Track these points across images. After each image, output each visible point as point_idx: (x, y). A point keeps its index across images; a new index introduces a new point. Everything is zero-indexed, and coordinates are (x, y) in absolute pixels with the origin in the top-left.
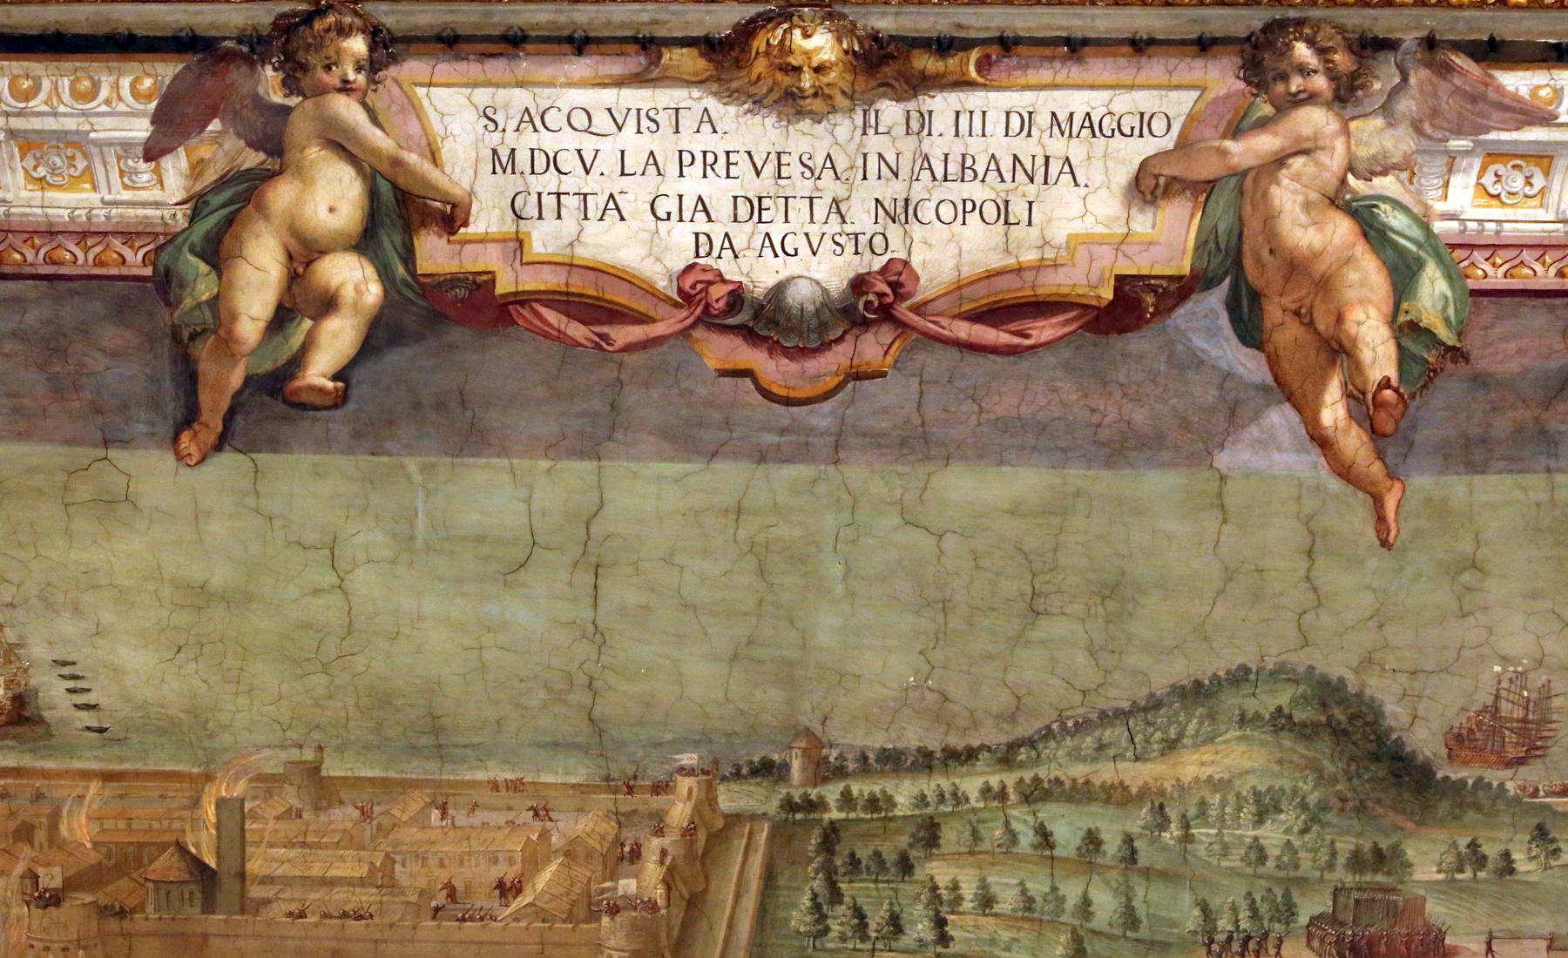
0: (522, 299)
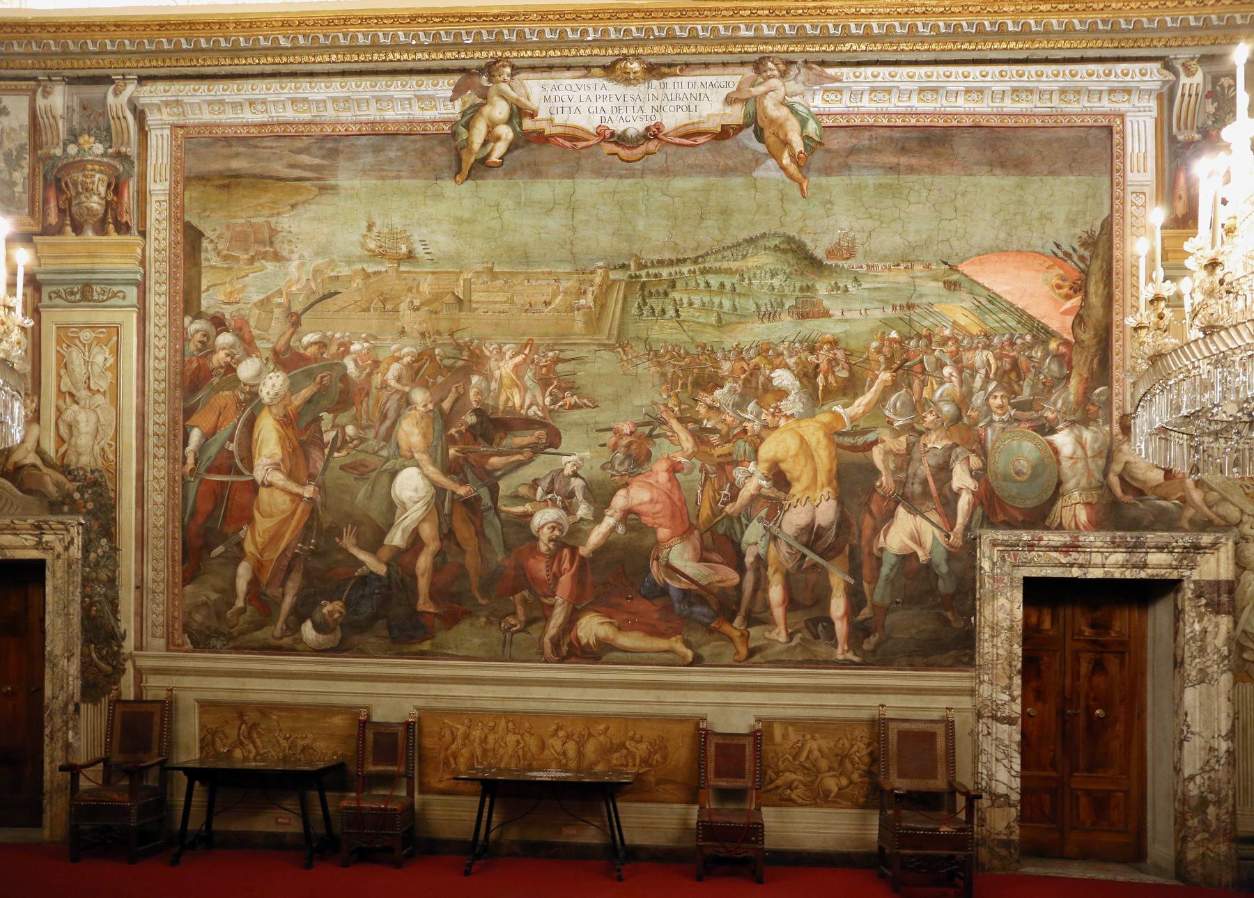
0: (552, 136)
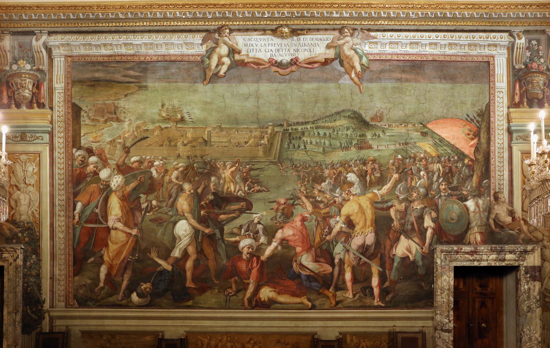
0: (248, 63)
